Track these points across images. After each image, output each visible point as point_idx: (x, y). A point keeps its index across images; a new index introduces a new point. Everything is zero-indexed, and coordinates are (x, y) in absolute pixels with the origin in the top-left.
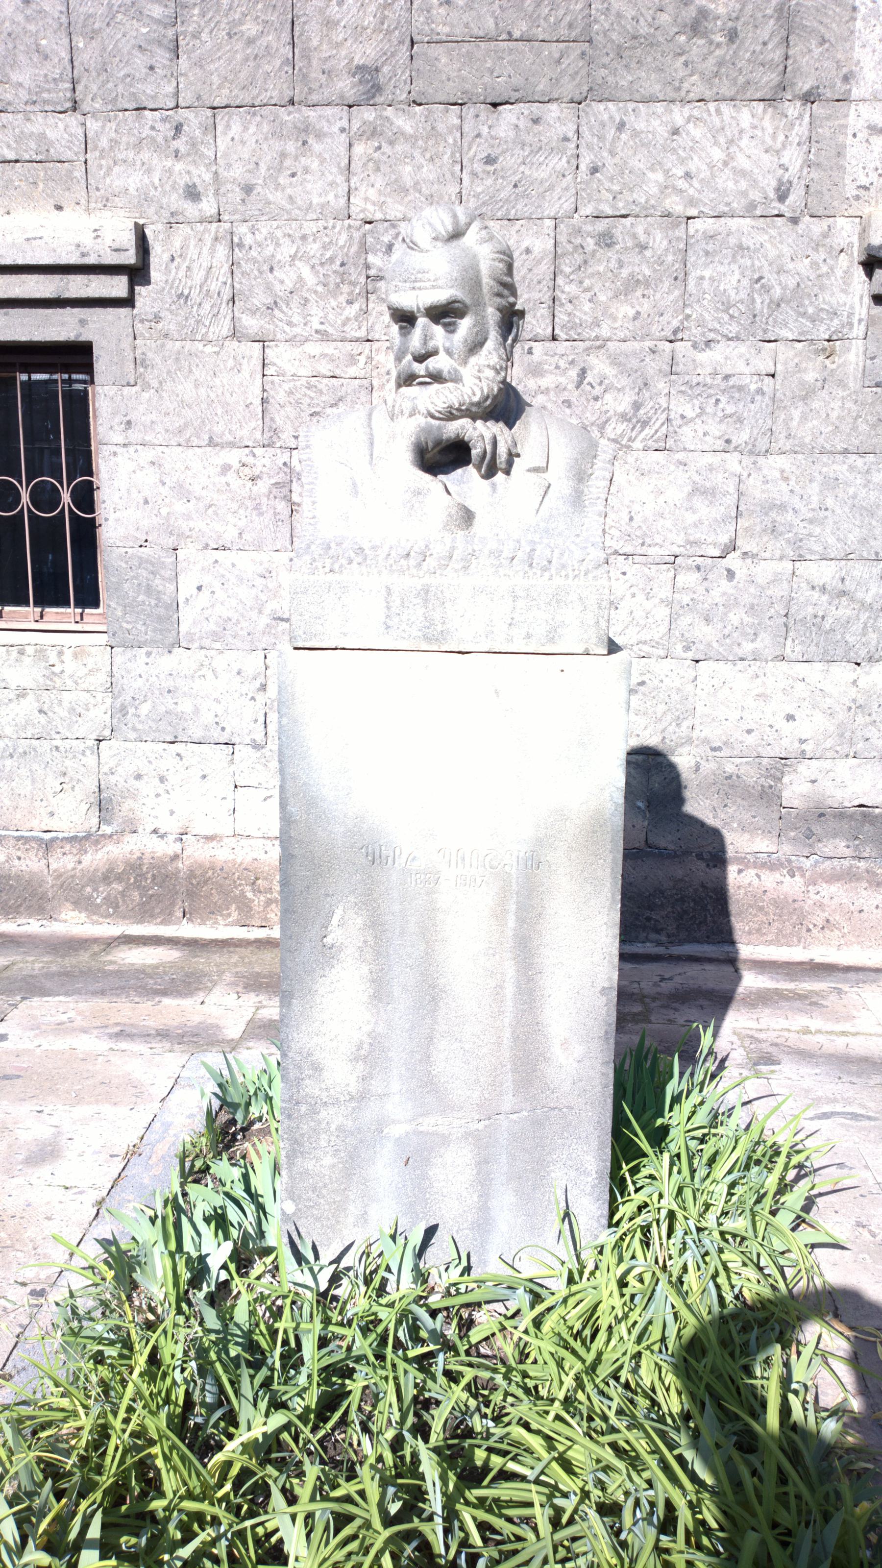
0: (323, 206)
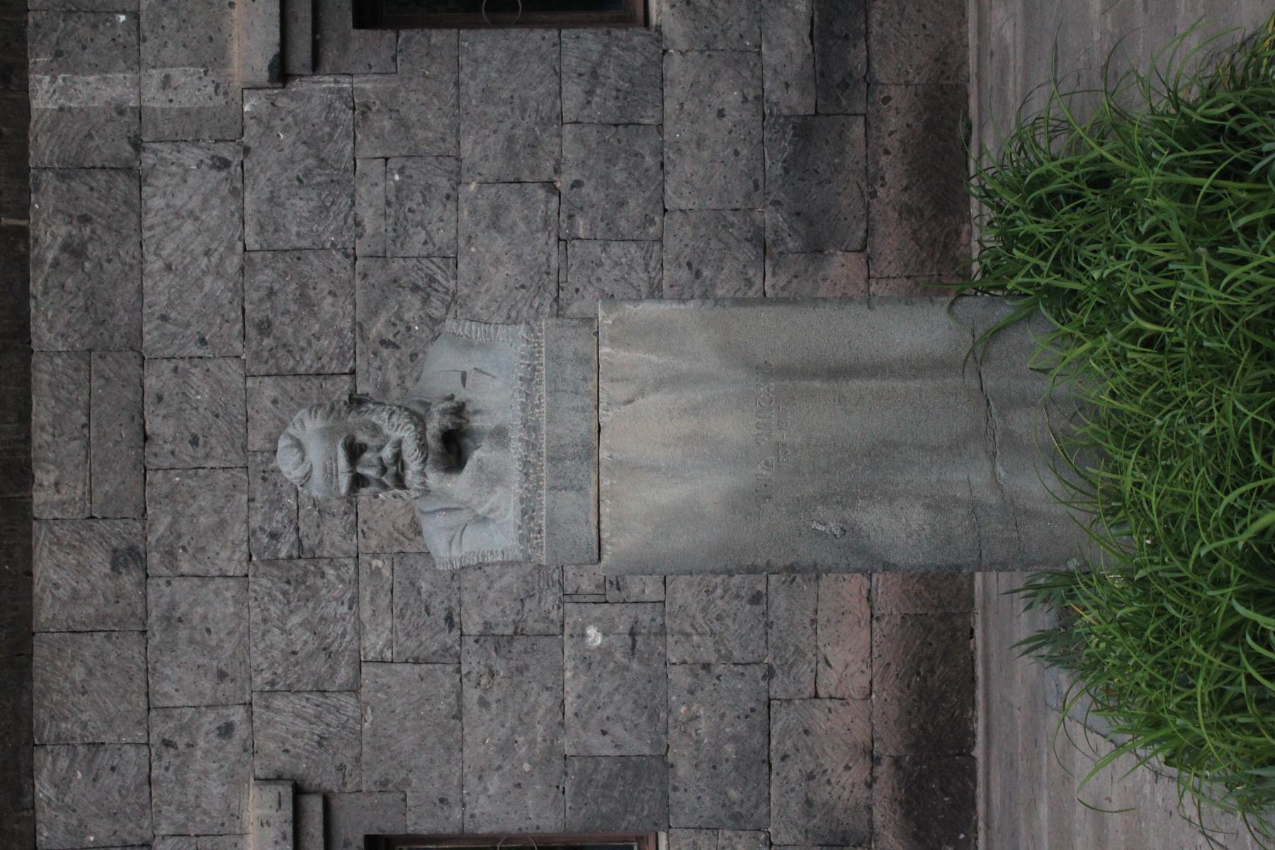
0: (236, 602)
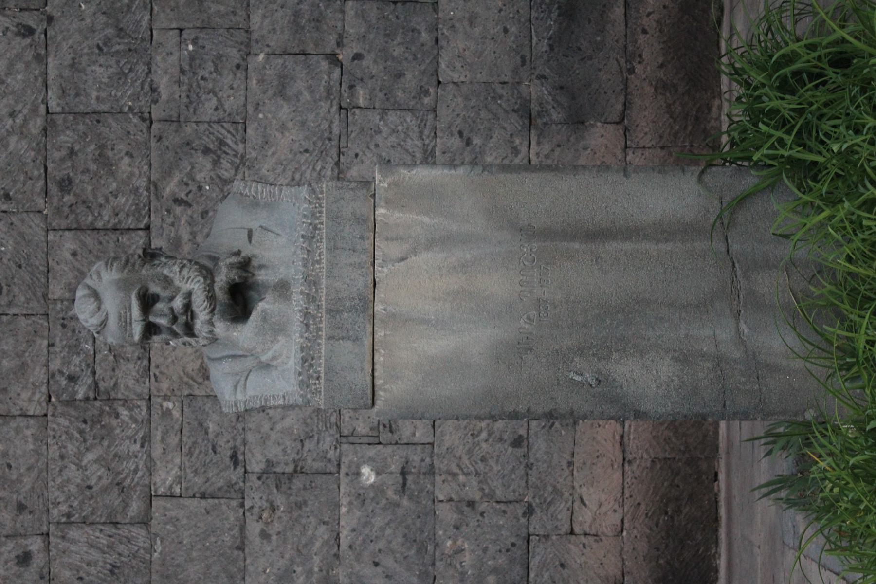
0: (36, 440)
